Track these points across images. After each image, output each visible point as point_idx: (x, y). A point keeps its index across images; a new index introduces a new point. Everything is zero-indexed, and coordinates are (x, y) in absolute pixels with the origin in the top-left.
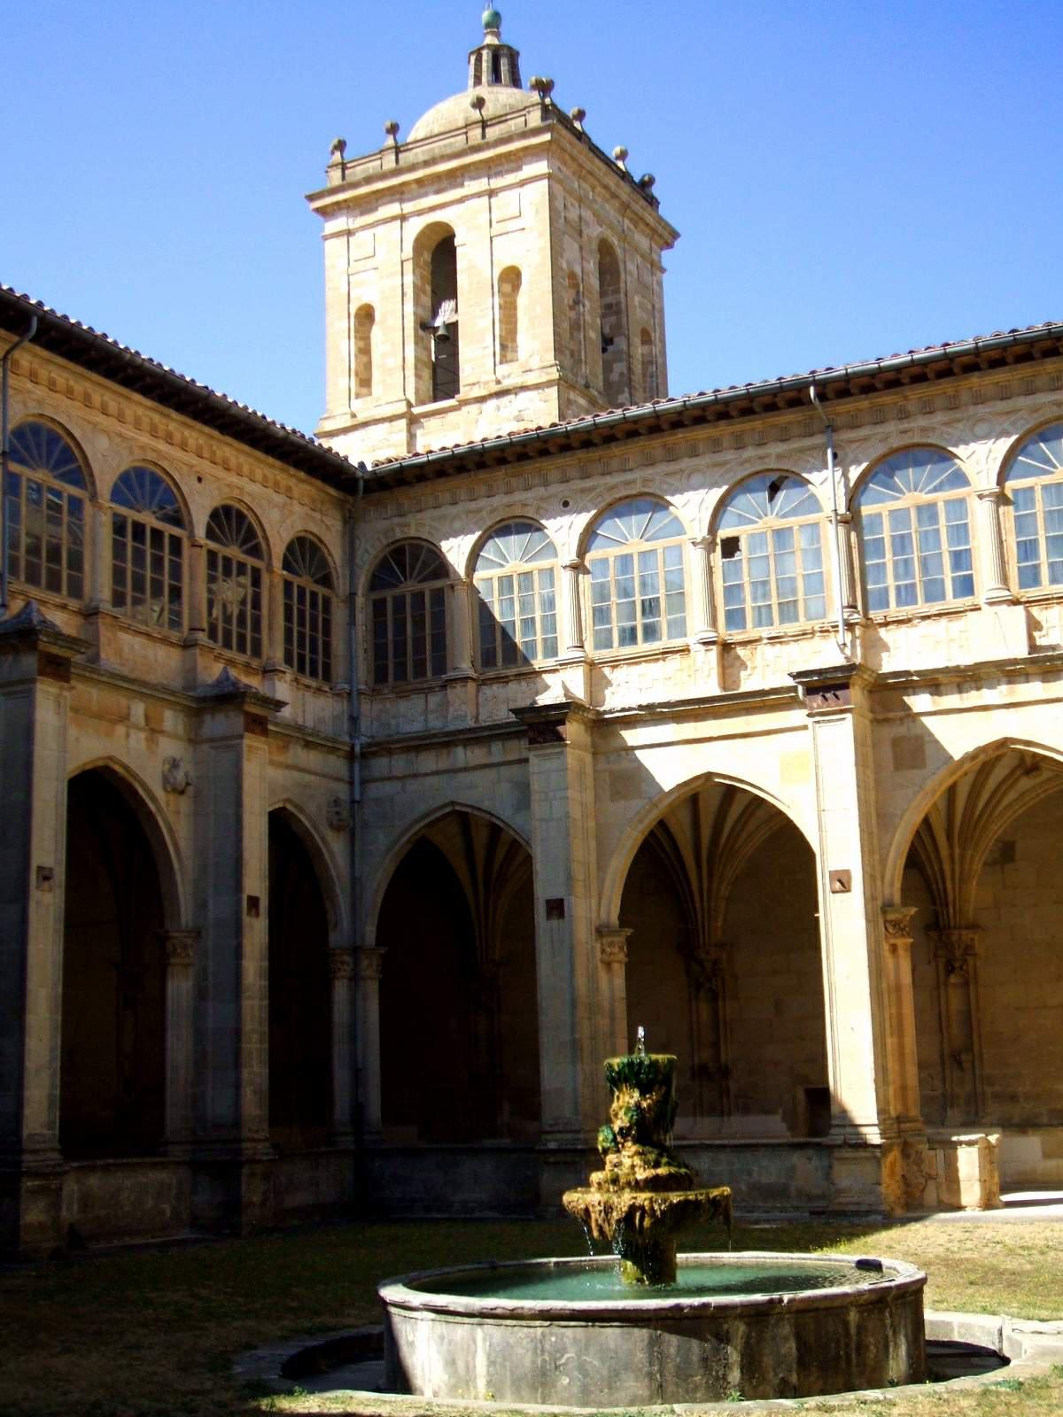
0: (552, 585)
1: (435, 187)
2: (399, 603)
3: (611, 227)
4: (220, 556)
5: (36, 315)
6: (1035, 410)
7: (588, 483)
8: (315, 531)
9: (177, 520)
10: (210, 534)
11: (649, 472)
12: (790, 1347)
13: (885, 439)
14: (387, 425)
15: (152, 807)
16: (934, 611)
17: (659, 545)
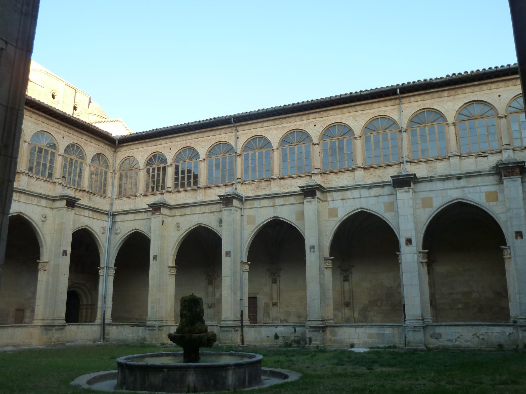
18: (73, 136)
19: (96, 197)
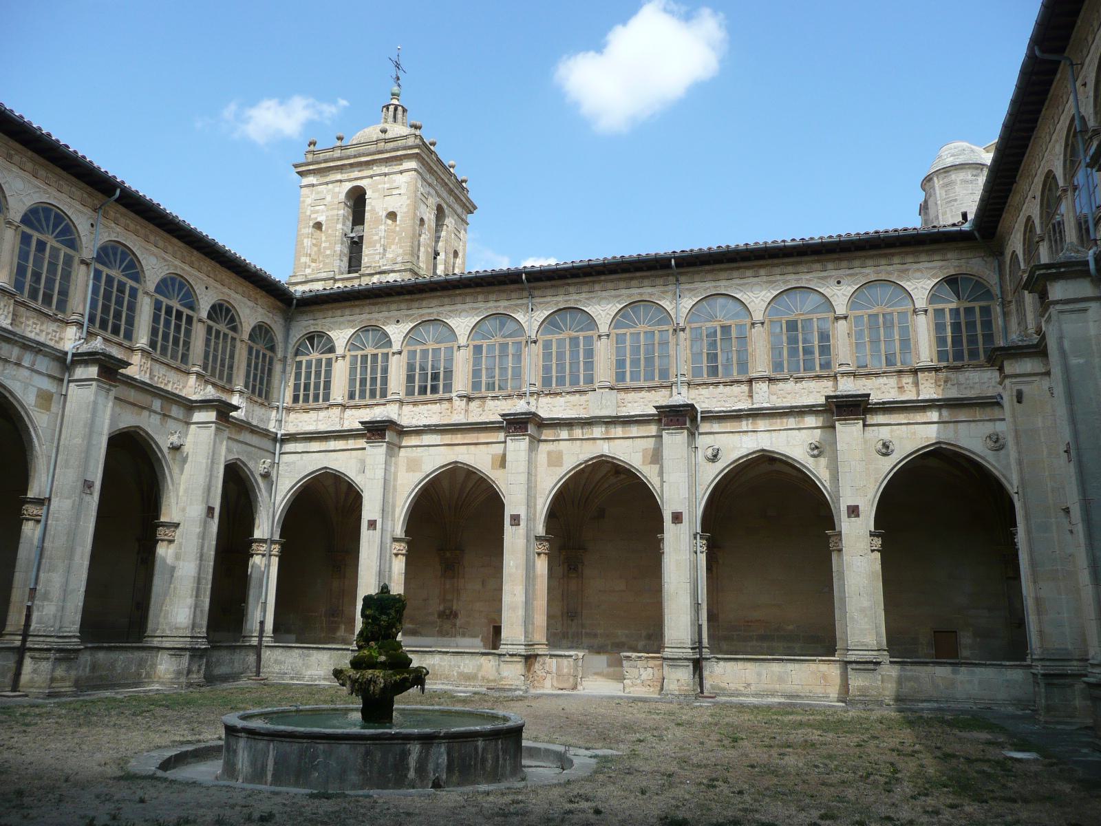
0: (387, 362)
1: (359, 169)
2: (309, 364)
3: (443, 199)
4: (214, 328)
5: (119, 187)
6: (629, 296)
7: (410, 312)
8: (269, 322)
9: (191, 307)
10: (210, 316)
11: (441, 309)
12: (444, 760)
13: (558, 302)
14: (323, 282)
15: (160, 455)
16: (573, 390)
17: (442, 346)
18: (863, 270)
19: (967, 374)
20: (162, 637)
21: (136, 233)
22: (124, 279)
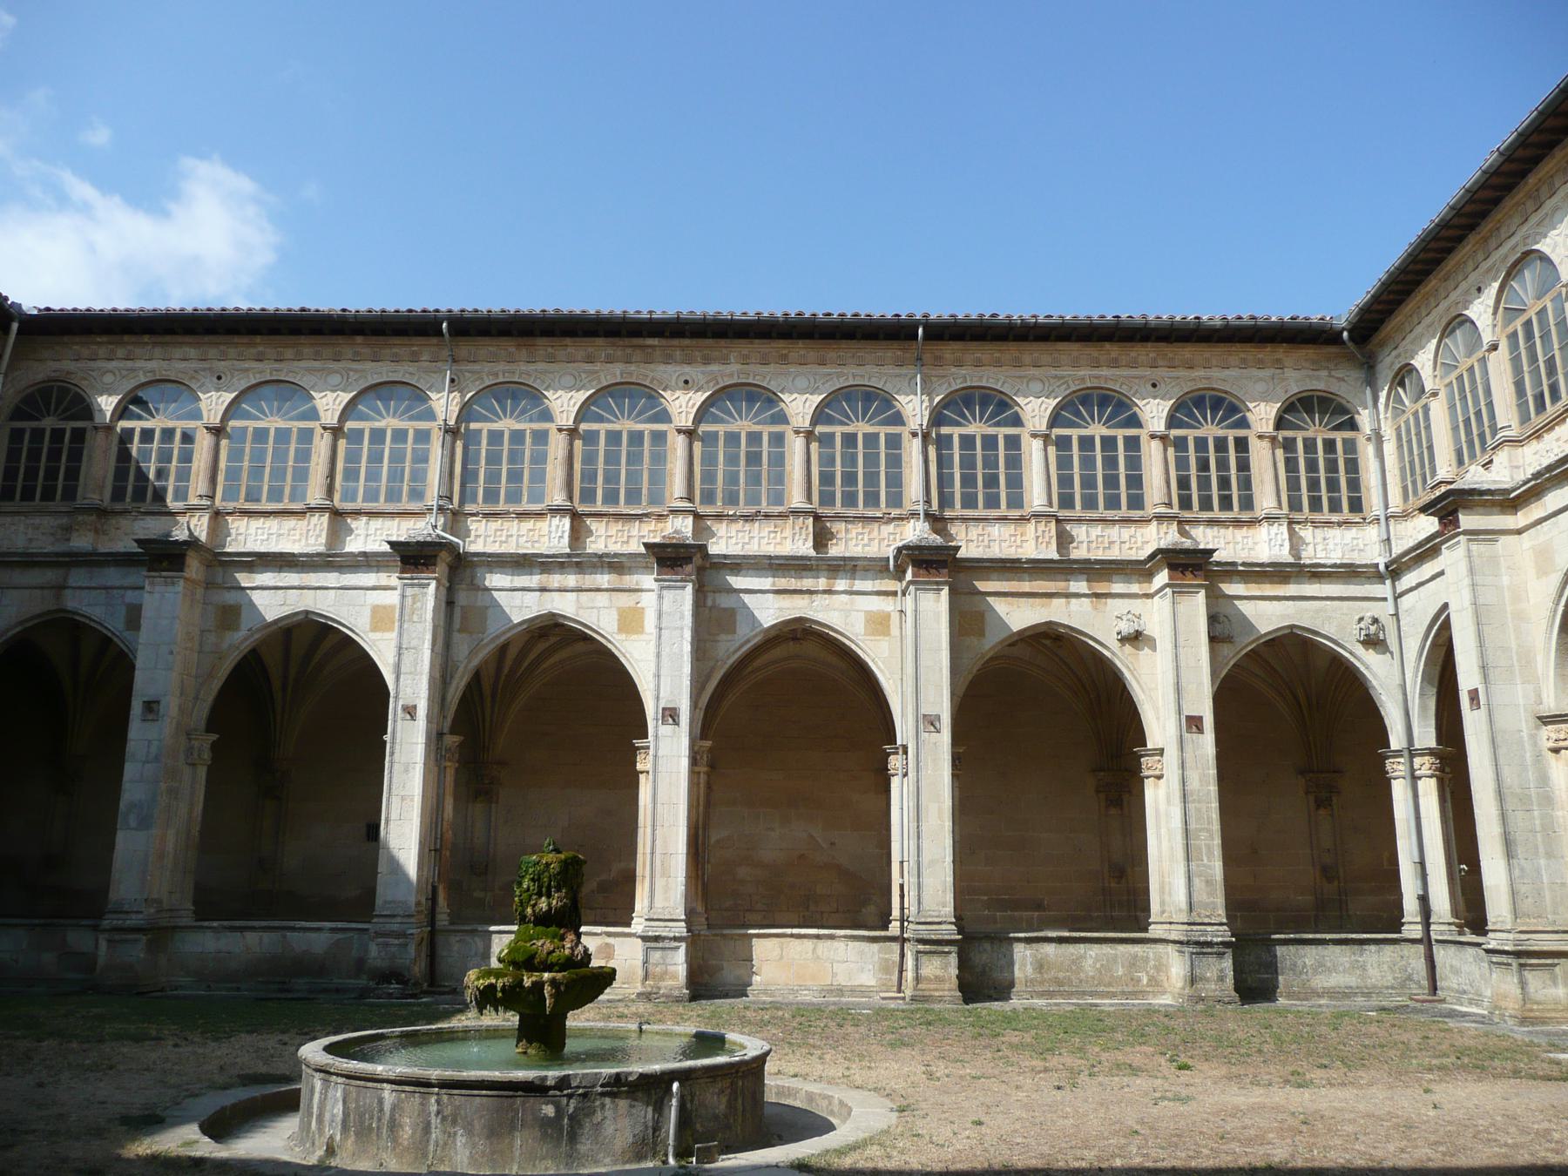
20: (1171, 923)
21: (998, 364)
22: (991, 431)
